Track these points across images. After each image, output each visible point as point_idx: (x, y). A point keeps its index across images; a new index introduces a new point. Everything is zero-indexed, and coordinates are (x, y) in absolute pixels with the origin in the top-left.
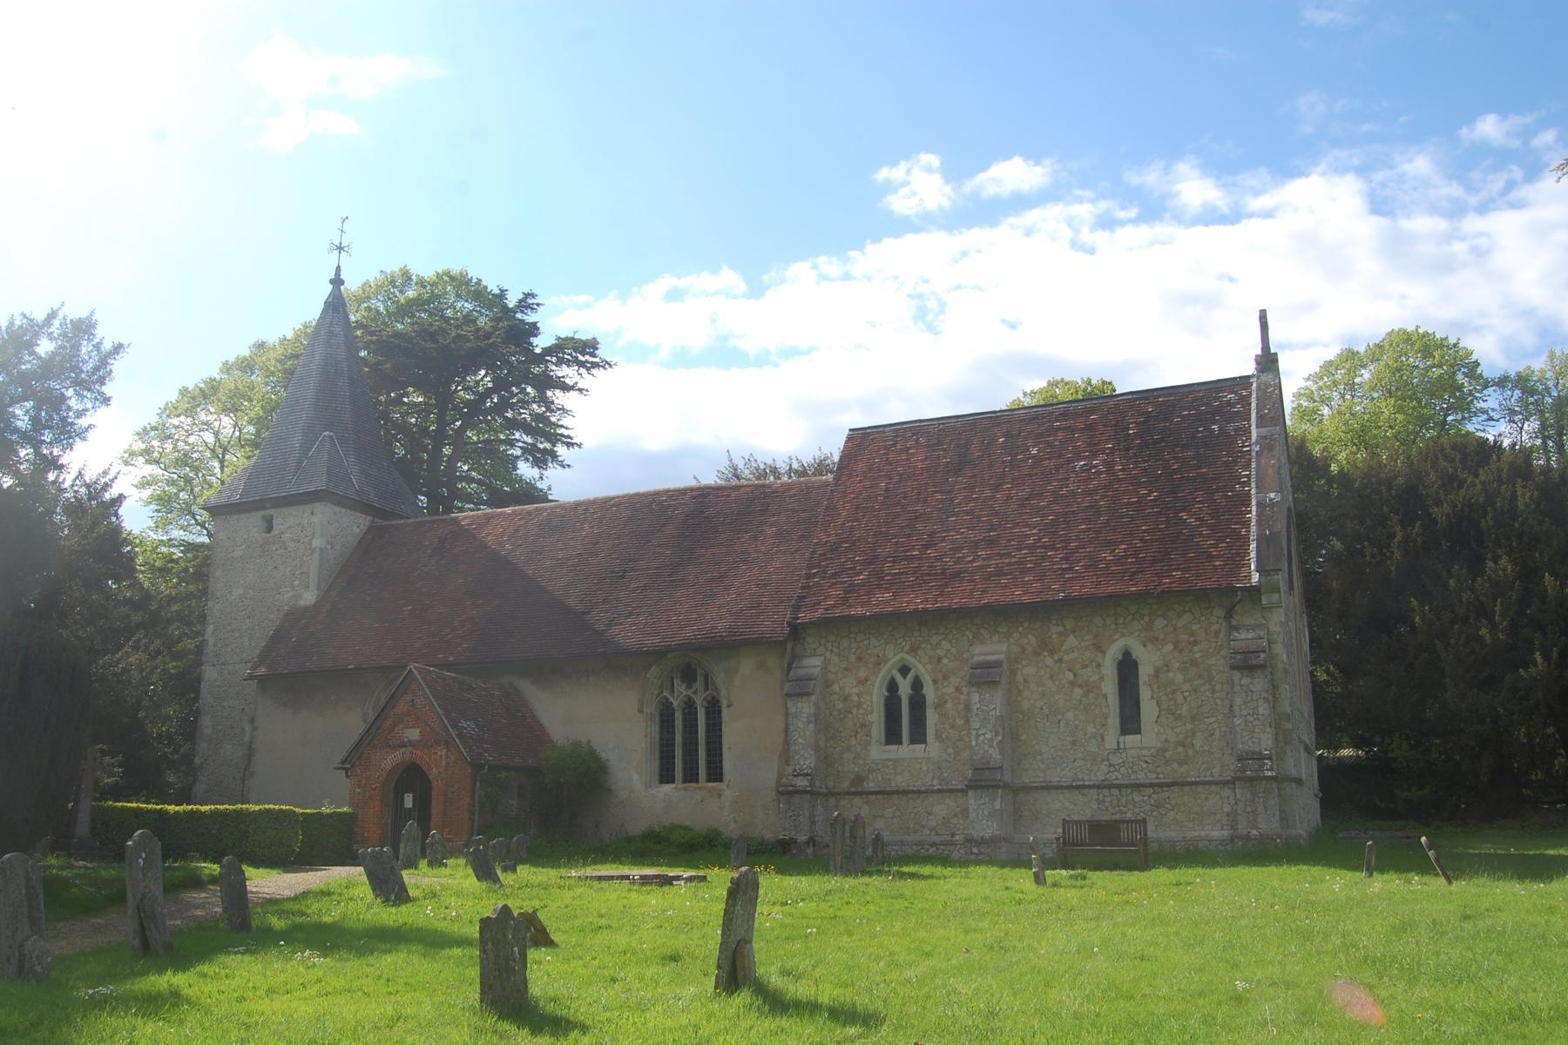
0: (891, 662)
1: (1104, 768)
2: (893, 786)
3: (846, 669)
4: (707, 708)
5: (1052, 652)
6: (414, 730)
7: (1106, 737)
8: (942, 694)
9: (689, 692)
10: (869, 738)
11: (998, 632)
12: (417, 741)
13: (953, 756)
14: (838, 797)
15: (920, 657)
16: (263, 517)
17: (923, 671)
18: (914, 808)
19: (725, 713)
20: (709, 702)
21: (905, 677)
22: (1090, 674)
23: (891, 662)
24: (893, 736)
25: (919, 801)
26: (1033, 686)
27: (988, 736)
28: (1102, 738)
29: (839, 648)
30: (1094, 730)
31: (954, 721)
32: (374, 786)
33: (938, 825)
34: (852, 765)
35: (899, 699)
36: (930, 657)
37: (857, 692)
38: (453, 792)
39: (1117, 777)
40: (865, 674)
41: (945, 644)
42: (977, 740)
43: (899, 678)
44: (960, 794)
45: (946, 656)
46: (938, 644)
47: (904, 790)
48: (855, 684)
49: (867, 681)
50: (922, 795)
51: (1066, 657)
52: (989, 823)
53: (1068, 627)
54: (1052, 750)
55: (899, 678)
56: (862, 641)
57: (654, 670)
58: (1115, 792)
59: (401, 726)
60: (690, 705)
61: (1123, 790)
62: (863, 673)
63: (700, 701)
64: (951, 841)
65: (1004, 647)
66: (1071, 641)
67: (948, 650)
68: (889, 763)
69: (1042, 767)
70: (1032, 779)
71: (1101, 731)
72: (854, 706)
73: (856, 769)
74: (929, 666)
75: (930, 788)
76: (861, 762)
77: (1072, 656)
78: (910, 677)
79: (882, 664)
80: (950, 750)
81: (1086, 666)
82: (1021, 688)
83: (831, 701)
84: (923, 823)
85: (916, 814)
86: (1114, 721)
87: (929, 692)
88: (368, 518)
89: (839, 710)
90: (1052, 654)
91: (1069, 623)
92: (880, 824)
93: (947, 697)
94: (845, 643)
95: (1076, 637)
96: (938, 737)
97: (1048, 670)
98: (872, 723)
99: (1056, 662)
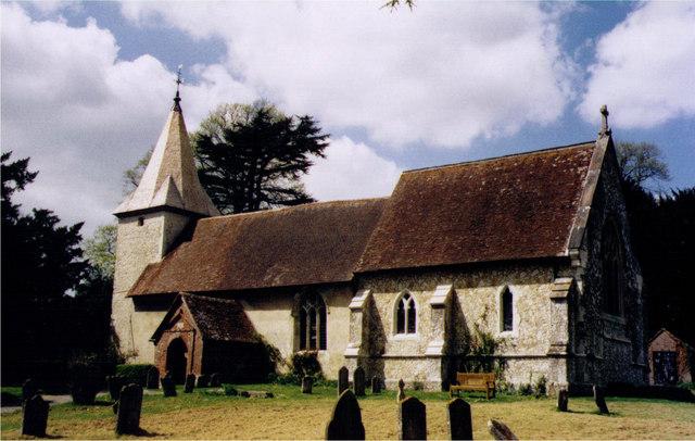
19: (328, 317)
24: (400, 329)
41: (425, 284)
43: (404, 300)
87: (417, 307)
94: (380, 283)
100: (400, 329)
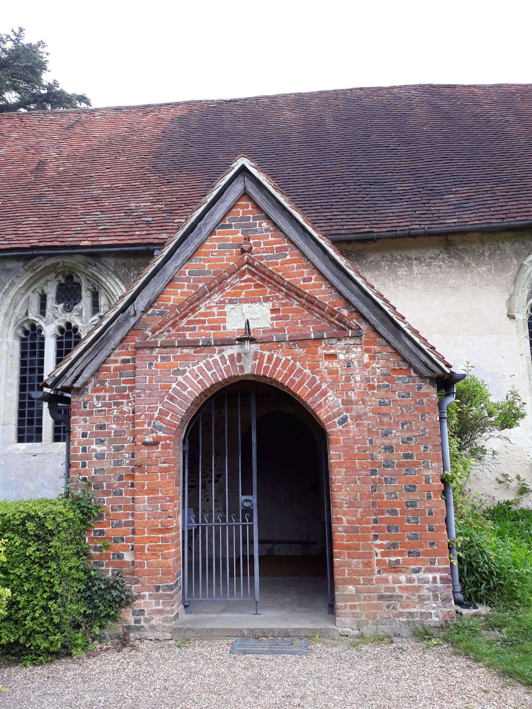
6: (256, 306)
32: (148, 439)
38: (389, 449)
59: (217, 298)
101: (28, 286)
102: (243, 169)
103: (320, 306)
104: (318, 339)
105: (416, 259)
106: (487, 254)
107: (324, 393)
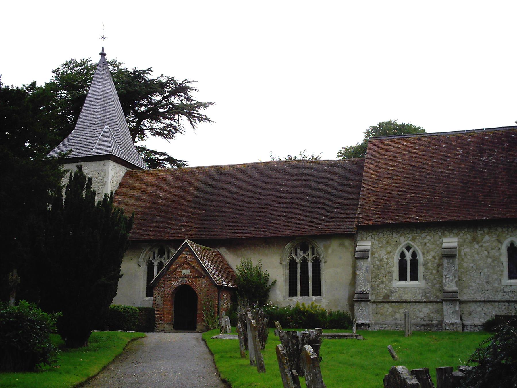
0: (402, 245)
1: (501, 294)
2: (404, 299)
3: (381, 247)
4: (312, 263)
5: (478, 243)
7: (502, 280)
8: (427, 259)
9: (305, 255)
10: (392, 278)
11: (453, 233)
12: (189, 275)
13: (431, 287)
14: (377, 303)
15: (417, 243)
16: (77, 166)
17: (418, 249)
18: (413, 309)
19: (323, 265)
20: (314, 260)
21: (408, 252)
22: (495, 253)
23: (402, 245)
24: (402, 277)
25: (415, 306)
26: (469, 257)
27: (451, 278)
28: (500, 281)
29: (378, 238)
30: (497, 277)
31: (432, 271)
33: (424, 317)
34: (384, 290)
35: (406, 261)
36: (421, 243)
37: (386, 257)
39: (507, 298)
40: (390, 249)
41: (428, 237)
42: (445, 280)
43: (406, 251)
44: (435, 303)
45: (428, 243)
46: (425, 237)
47: (409, 301)
48: (385, 254)
49: (391, 253)
50: (417, 304)
51: (484, 245)
52: (453, 316)
53: (486, 232)
54: (477, 285)
55: (406, 251)
56: (389, 235)
57: (289, 245)
58: (507, 304)
60: (304, 263)
61: (510, 304)
62: (389, 249)
63: (310, 259)
64: (431, 323)
65: (456, 240)
66: (487, 238)
67: (430, 240)
68: (401, 289)
69: (473, 292)
70: (468, 298)
71: (500, 277)
72: (385, 264)
73: (386, 292)
74: (420, 247)
75: (421, 300)
76: (388, 288)
77: (487, 244)
78: (411, 251)
79: (398, 246)
80: (430, 284)
81: (493, 249)
82: (463, 258)
83: (374, 261)
84: (418, 315)
85: (414, 312)
86: (506, 273)
87: (421, 258)
88: (126, 168)
89: (378, 265)
90: (478, 243)
91: (486, 230)
92: (398, 316)
93: (429, 261)
94: (381, 235)
95: (489, 236)
96: (425, 278)
97: (476, 250)
98: (393, 271)
99: (480, 247)
100: (402, 277)
101: (150, 250)
102: (186, 242)
103: (198, 271)
104: (197, 277)
105: (257, 245)
106: (276, 244)
107: (197, 288)
